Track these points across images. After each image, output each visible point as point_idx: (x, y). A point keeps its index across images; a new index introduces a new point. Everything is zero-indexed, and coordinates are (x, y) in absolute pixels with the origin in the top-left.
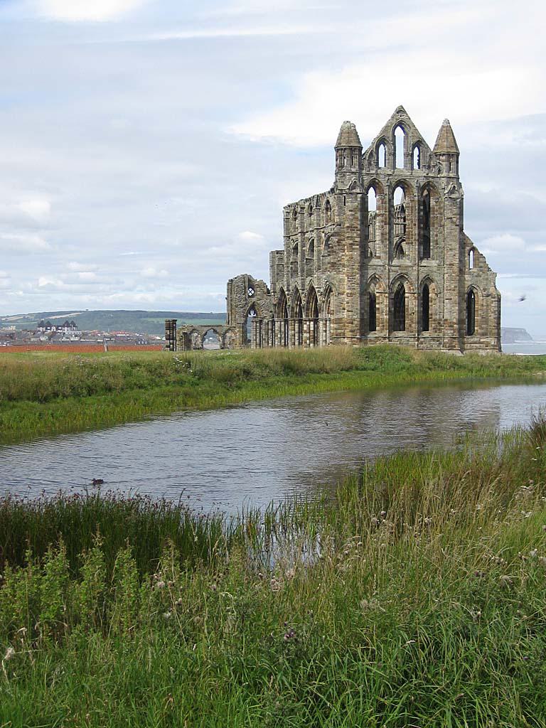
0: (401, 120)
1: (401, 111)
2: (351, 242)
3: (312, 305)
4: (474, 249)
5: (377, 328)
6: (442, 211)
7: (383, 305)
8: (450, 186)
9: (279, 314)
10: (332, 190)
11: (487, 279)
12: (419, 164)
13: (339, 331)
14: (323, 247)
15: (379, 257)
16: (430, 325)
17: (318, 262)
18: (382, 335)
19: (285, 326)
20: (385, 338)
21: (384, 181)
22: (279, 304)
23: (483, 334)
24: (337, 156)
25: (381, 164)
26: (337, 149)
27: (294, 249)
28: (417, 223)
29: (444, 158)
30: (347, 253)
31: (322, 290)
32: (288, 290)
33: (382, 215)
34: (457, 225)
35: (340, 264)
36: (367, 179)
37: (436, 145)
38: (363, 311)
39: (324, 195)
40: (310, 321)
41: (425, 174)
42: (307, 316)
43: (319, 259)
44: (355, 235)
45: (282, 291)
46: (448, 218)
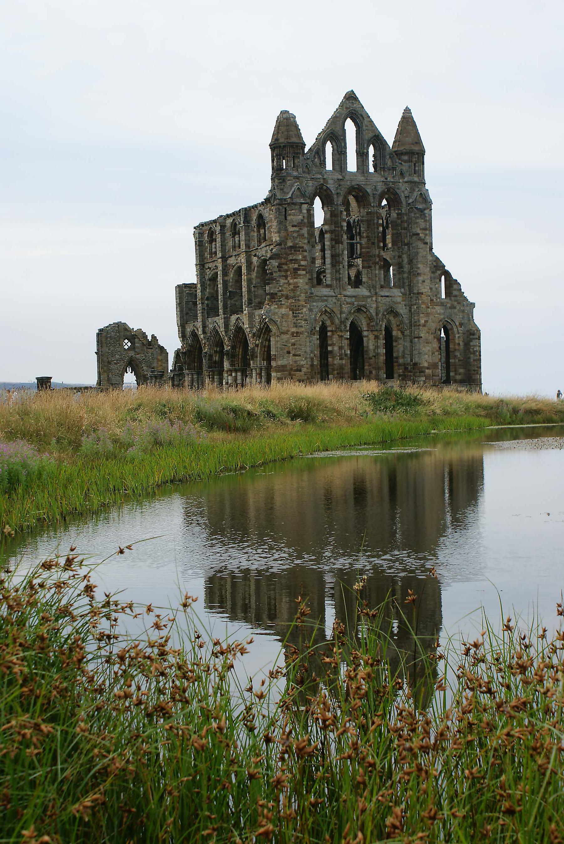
1: (351, 97)
2: (296, 266)
3: (239, 351)
4: (447, 274)
6: (406, 225)
7: (340, 345)
8: (415, 194)
9: (189, 365)
10: (267, 200)
11: (463, 311)
12: (375, 166)
14: (254, 274)
16: (395, 371)
17: (248, 294)
19: (198, 380)
21: (331, 186)
22: (189, 351)
24: (272, 156)
25: (329, 166)
26: (274, 147)
27: (210, 280)
28: (376, 241)
29: (406, 158)
30: (291, 281)
31: (255, 330)
32: (204, 332)
33: (331, 232)
35: (282, 295)
36: (311, 186)
37: (394, 142)
38: (312, 355)
39: (255, 207)
40: (236, 371)
41: (383, 179)
42: (232, 365)
43: (249, 291)
44: (300, 257)
45: (194, 335)
46: (414, 235)
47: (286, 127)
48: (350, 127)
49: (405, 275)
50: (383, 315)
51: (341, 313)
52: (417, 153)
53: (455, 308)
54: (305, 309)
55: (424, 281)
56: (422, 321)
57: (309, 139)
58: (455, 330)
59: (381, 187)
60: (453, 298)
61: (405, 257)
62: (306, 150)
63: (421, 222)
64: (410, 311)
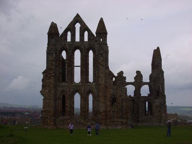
0: (78, 19)
1: (78, 16)
5: (66, 115)
6: (97, 59)
11: (122, 91)
13: (46, 116)
15: (67, 82)
18: (67, 118)
20: (68, 119)
21: (67, 47)
23: (120, 118)
25: (69, 39)
29: (98, 35)
33: (68, 63)
34: (103, 66)
35: (47, 86)
47: (53, 28)
48: (78, 26)
49: (97, 78)
50: (87, 92)
51: (70, 91)
52: (102, 33)
53: (118, 90)
54: (53, 91)
55: (102, 80)
56: (101, 95)
57: (61, 31)
58: (118, 98)
59: (87, 46)
60: (117, 86)
61: (96, 71)
62: (60, 35)
63: (102, 59)
64: (98, 91)
